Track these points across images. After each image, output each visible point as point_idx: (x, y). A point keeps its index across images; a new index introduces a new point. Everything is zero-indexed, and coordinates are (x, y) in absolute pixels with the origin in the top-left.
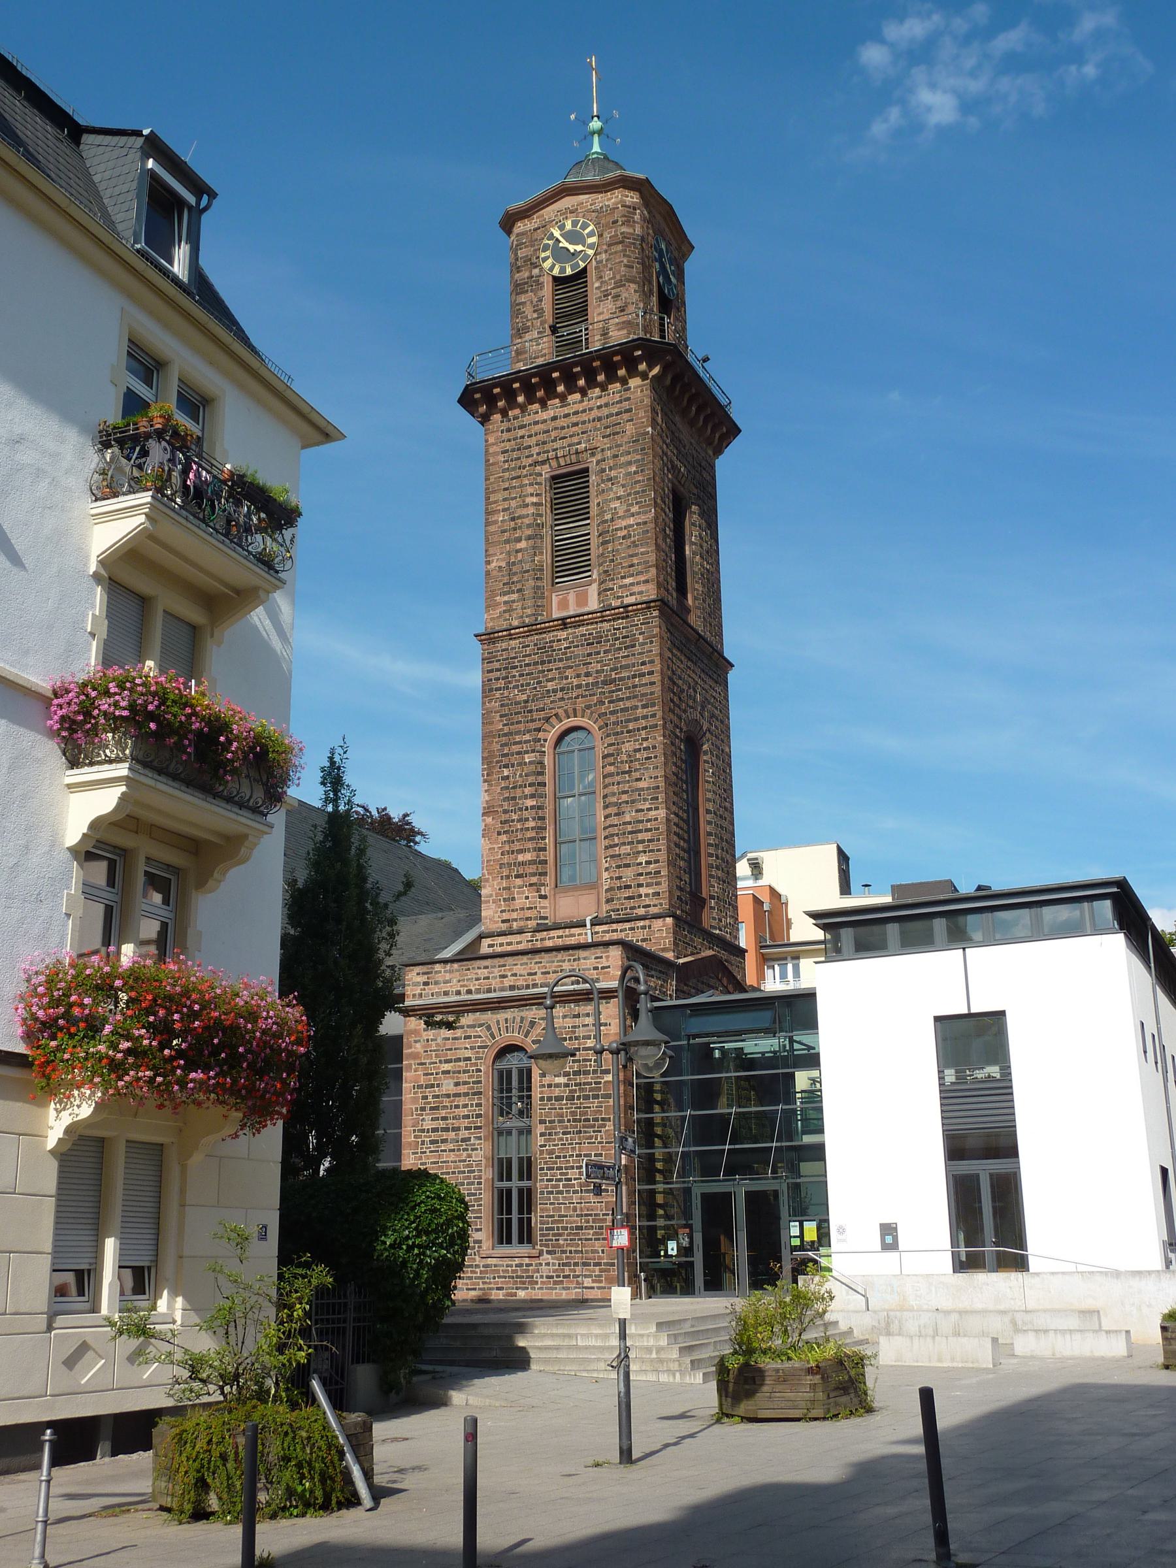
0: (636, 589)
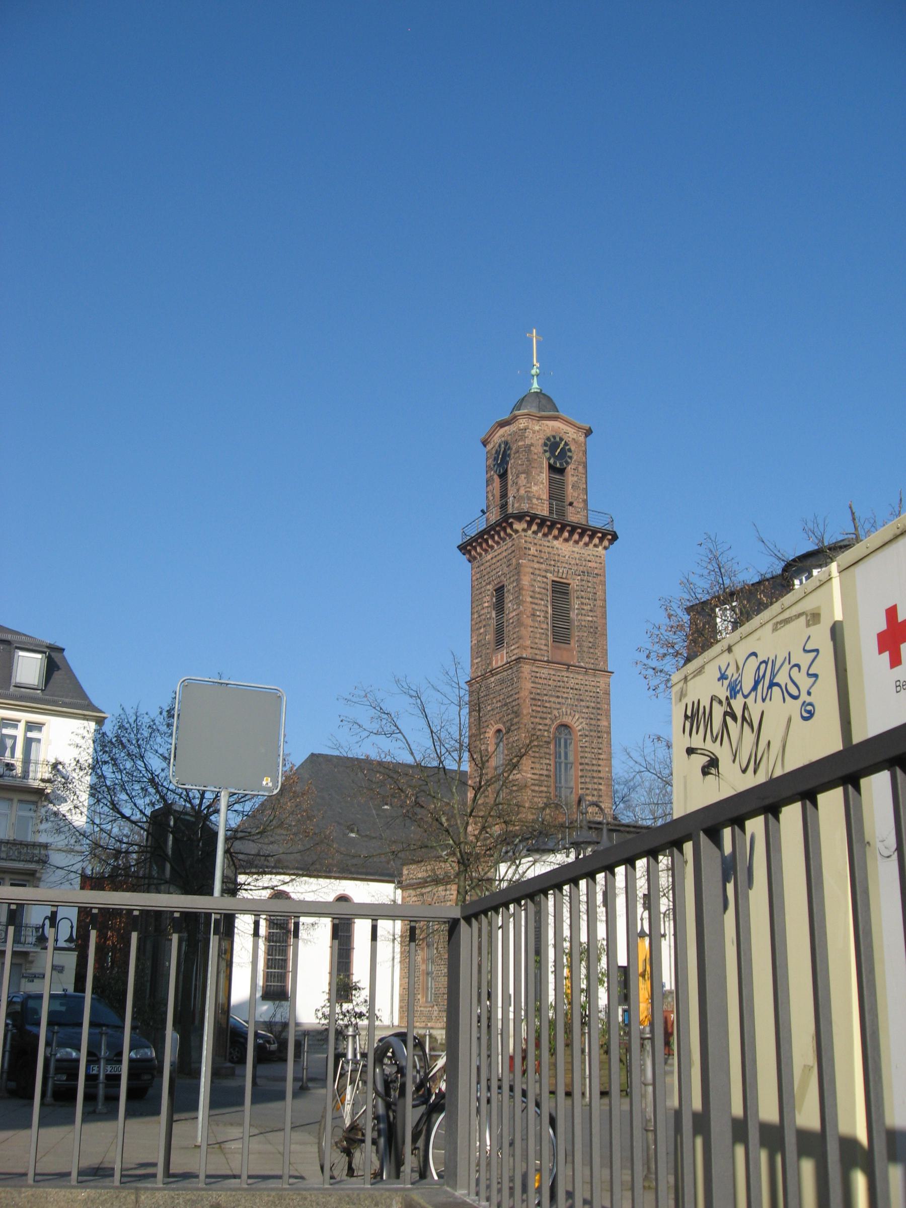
0: (515, 652)
